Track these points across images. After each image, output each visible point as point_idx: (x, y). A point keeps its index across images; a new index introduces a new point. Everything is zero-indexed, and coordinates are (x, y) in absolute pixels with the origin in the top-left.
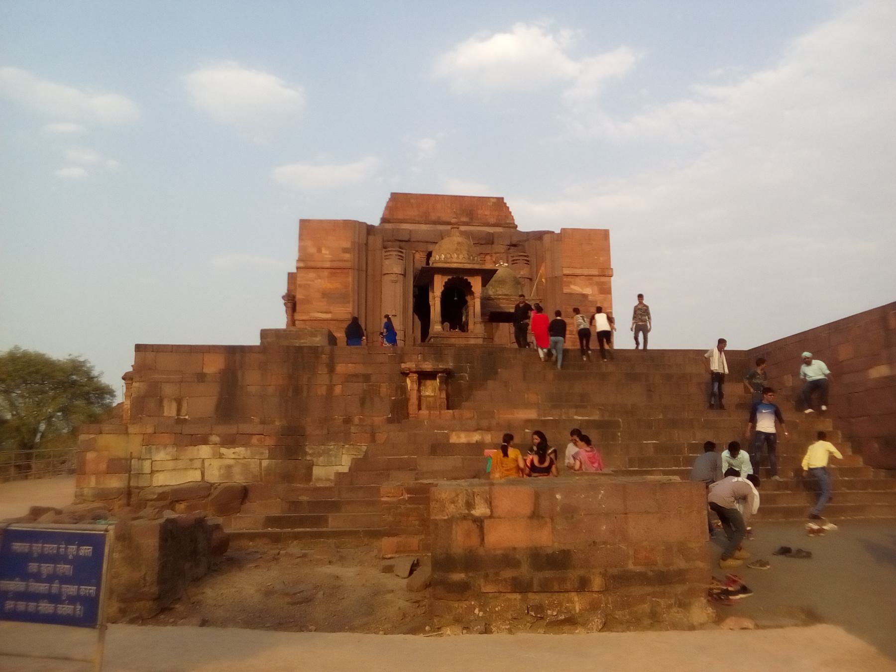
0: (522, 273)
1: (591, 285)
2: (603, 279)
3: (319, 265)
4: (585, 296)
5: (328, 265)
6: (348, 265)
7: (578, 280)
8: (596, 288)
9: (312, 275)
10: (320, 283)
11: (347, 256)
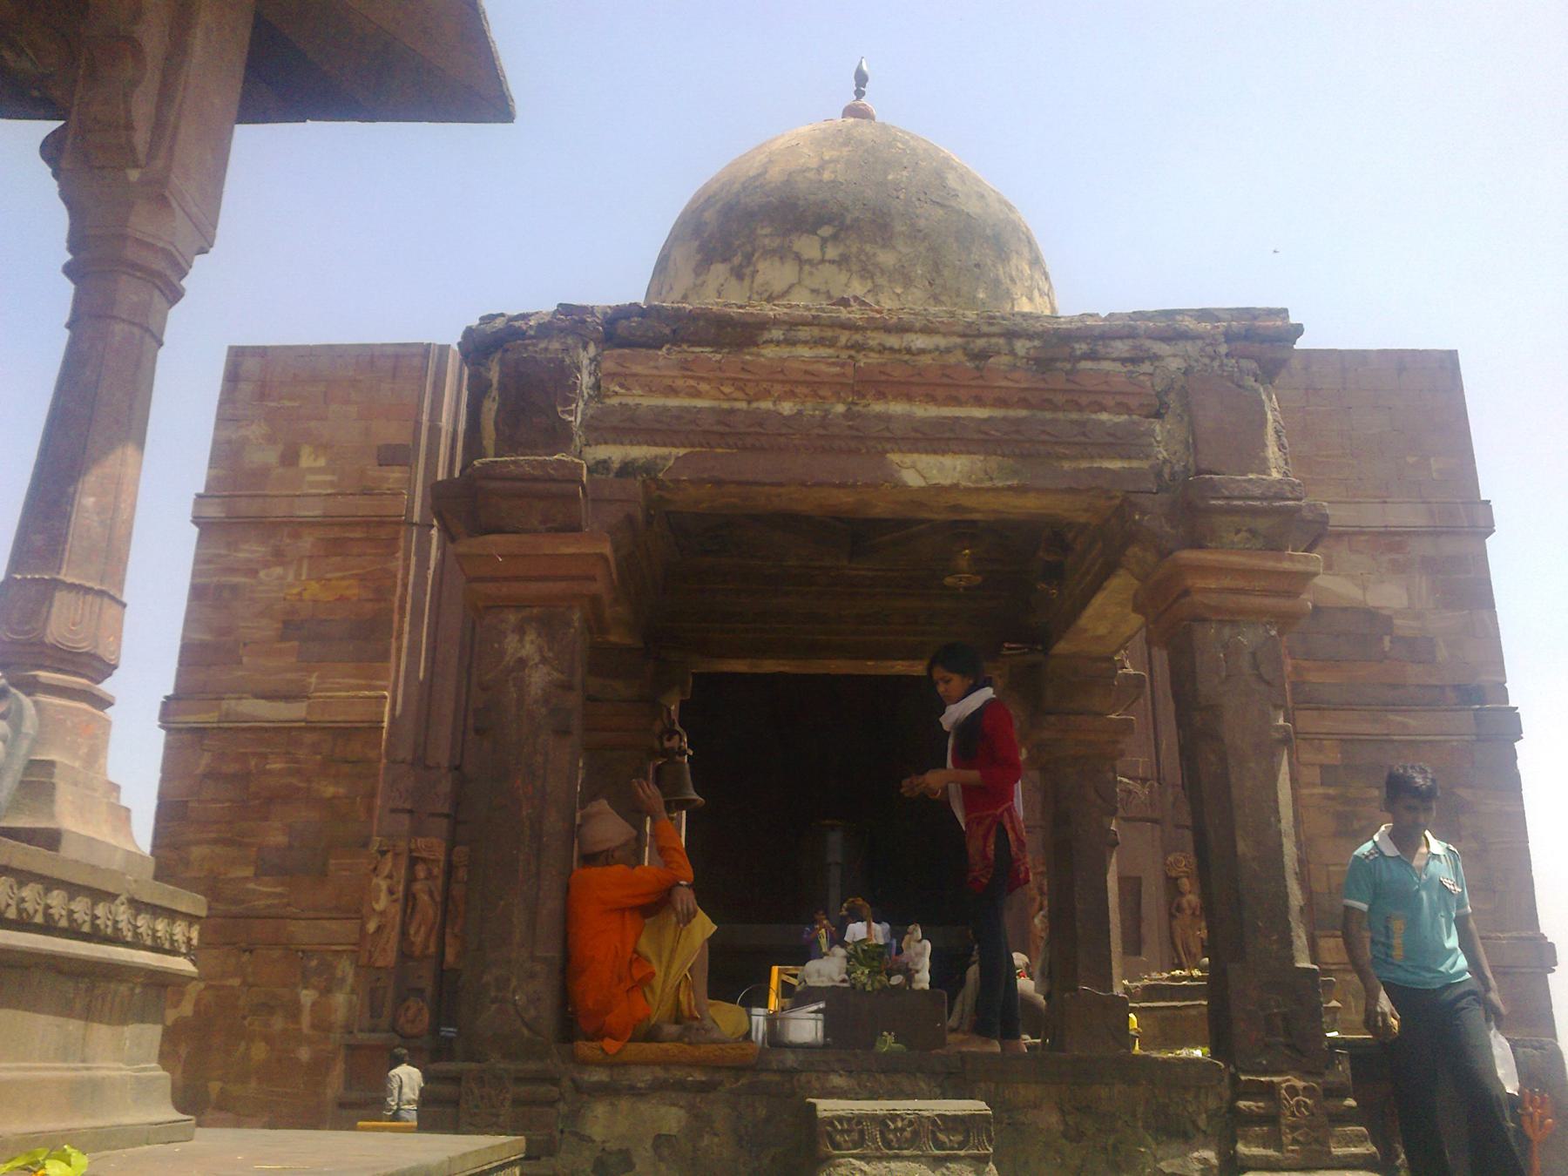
5: (312, 510)
11: (395, 474)
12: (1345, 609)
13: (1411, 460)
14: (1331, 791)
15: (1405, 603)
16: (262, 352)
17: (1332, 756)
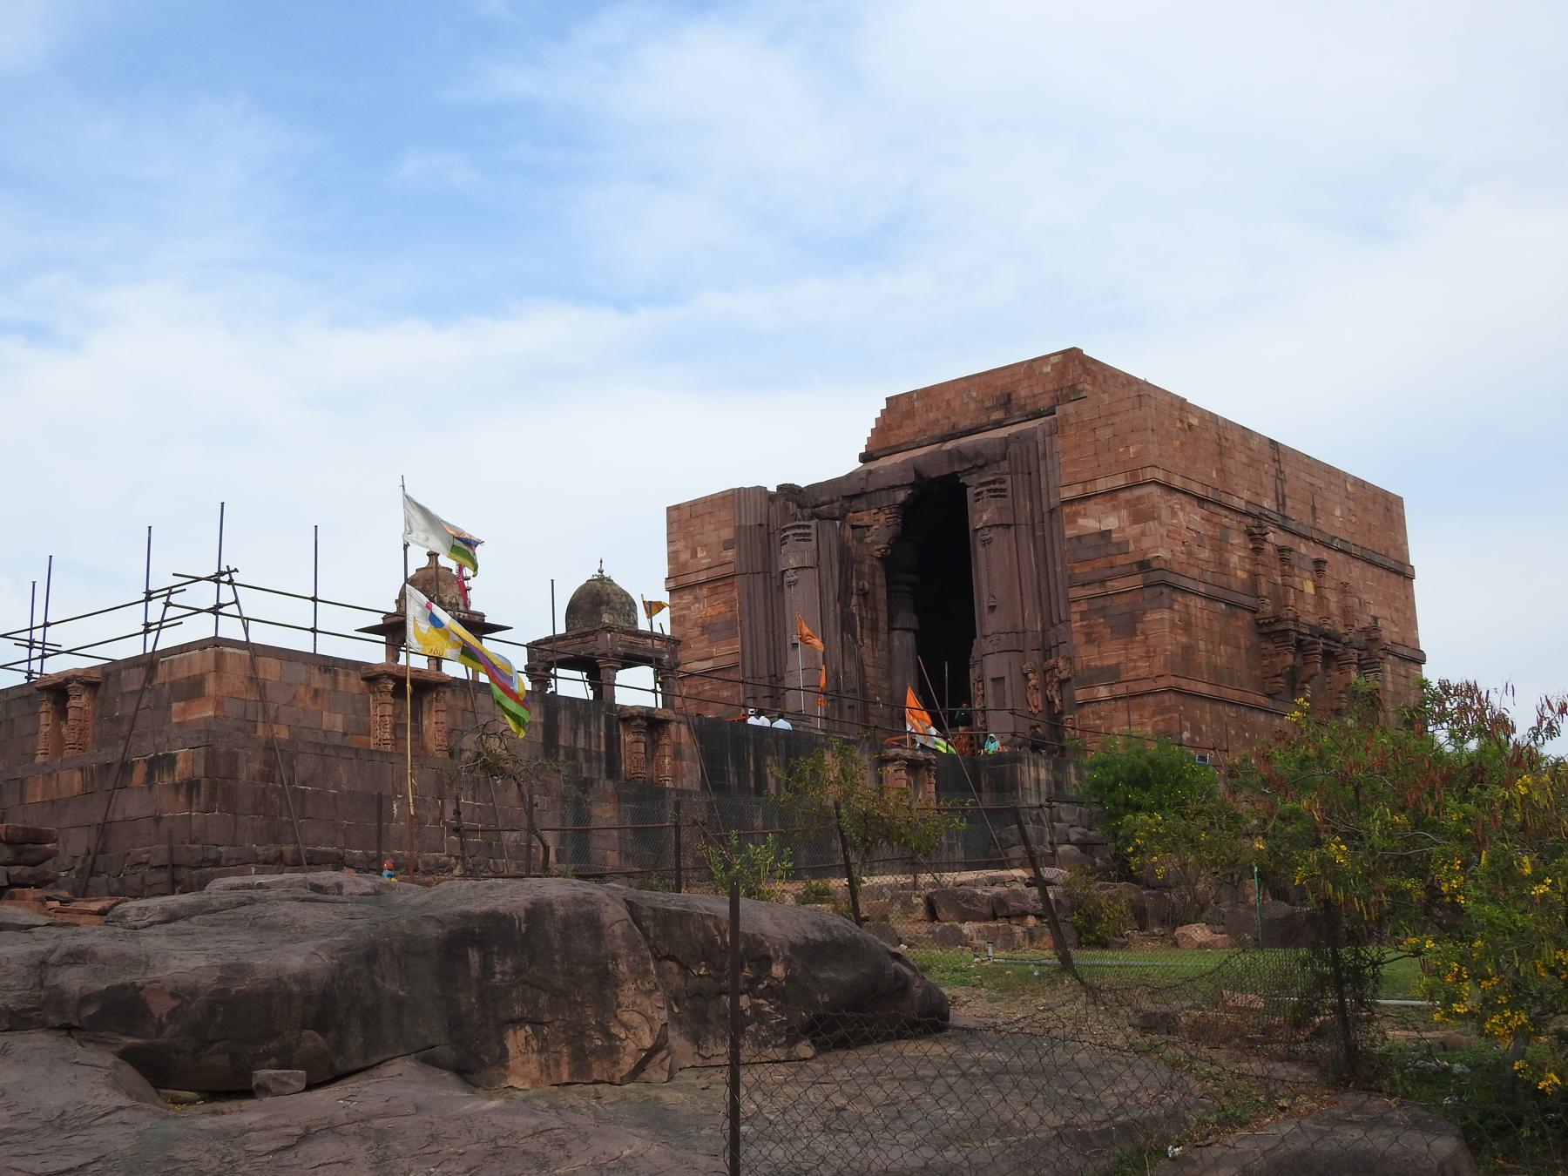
1: (1115, 508)
3: (692, 579)
5: (703, 577)
6: (730, 569)
7: (1091, 506)
8: (1124, 513)
9: (687, 598)
10: (702, 608)
11: (730, 554)
16: (677, 507)
17: (1084, 606)
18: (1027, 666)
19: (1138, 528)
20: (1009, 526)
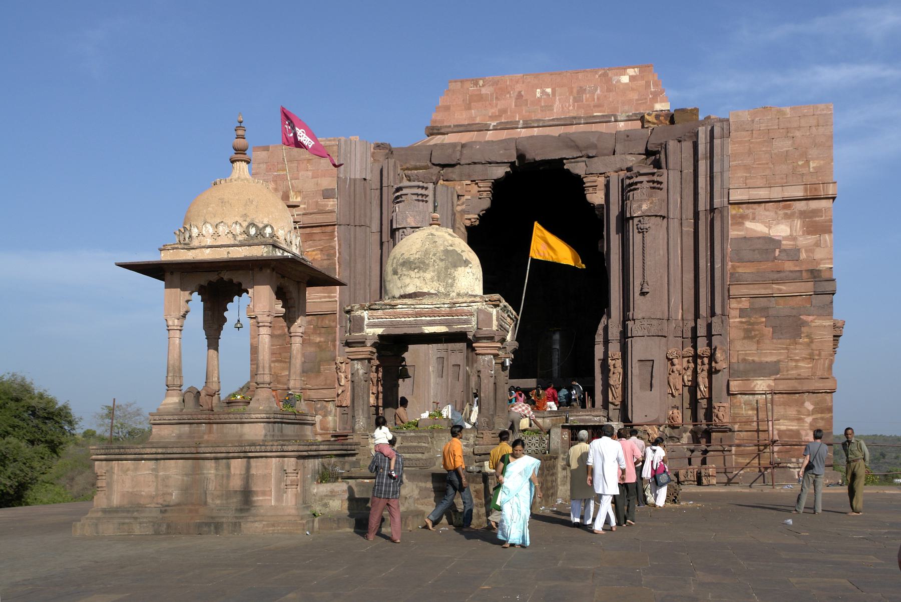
0: (644, 207)
1: (787, 217)
2: (814, 205)
4: (771, 243)
7: (759, 209)
8: (798, 223)
12: (759, 238)
13: (800, 163)
14: (744, 320)
15: (788, 233)
17: (745, 304)
18: (673, 351)
19: (811, 239)
20: (664, 217)
